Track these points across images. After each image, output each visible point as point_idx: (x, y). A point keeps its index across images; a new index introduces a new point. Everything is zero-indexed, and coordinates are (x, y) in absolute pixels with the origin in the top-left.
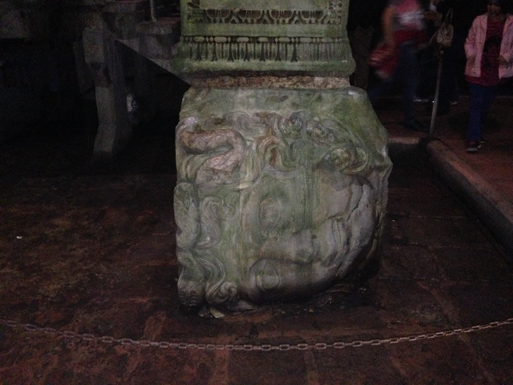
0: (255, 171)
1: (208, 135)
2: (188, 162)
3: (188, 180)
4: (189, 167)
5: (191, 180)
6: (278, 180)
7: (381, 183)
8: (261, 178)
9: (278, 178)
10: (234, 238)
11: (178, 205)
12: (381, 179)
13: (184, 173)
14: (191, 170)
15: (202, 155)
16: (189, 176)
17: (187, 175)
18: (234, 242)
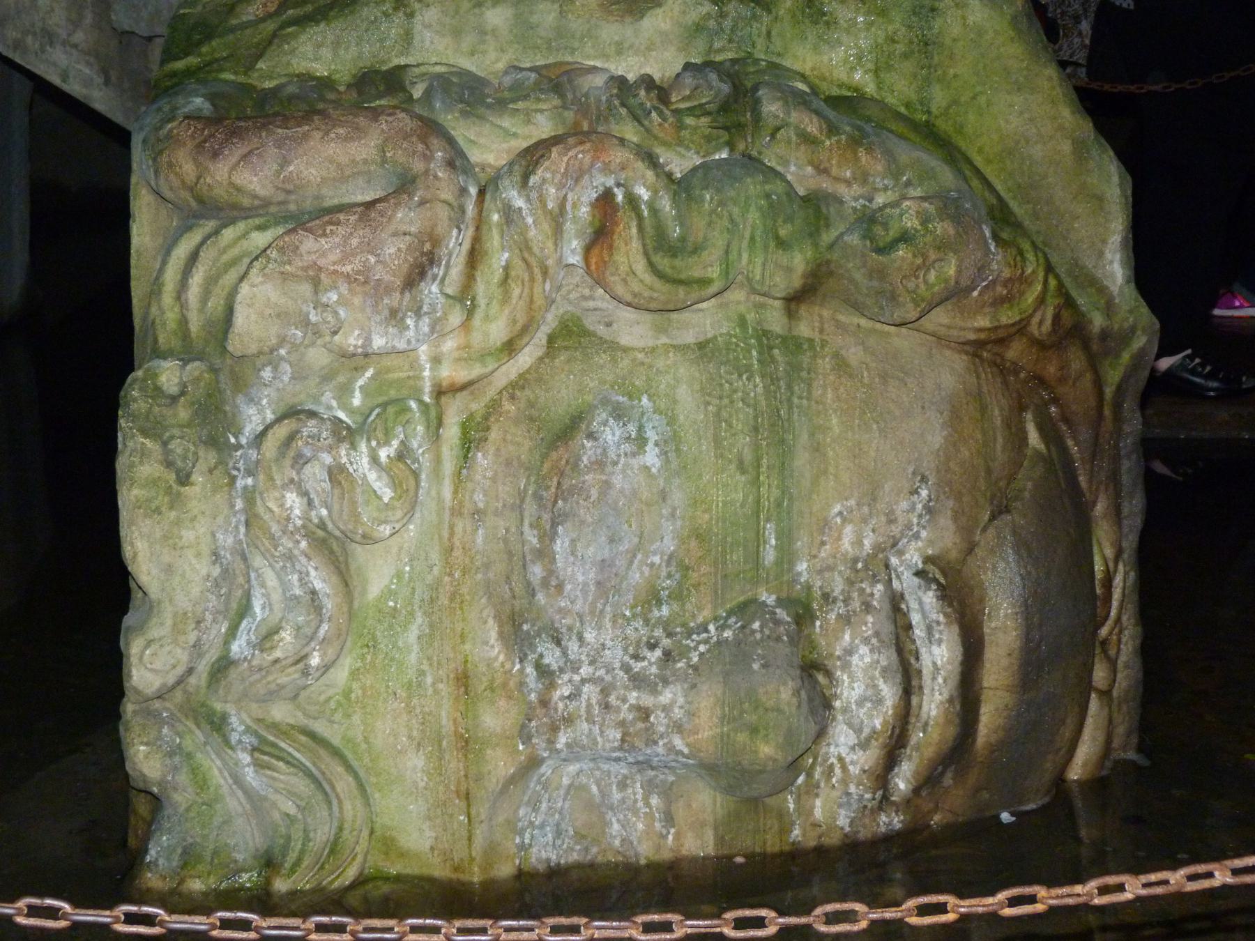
0: (516, 292)
1: (292, 123)
2: (194, 257)
3: (187, 353)
4: (197, 280)
5: (213, 342)
6: (625, 350)
7: (1107, 412)
8: (541, 337)
9: (625, 340)
10: (412, 635)
11: (139, 470)
12: (1109, 392)
13: (171, 316)
14: (204, 299)
15: (257, 221)
16: (194, 327)
17: (183, 321)
18: (413, 658)
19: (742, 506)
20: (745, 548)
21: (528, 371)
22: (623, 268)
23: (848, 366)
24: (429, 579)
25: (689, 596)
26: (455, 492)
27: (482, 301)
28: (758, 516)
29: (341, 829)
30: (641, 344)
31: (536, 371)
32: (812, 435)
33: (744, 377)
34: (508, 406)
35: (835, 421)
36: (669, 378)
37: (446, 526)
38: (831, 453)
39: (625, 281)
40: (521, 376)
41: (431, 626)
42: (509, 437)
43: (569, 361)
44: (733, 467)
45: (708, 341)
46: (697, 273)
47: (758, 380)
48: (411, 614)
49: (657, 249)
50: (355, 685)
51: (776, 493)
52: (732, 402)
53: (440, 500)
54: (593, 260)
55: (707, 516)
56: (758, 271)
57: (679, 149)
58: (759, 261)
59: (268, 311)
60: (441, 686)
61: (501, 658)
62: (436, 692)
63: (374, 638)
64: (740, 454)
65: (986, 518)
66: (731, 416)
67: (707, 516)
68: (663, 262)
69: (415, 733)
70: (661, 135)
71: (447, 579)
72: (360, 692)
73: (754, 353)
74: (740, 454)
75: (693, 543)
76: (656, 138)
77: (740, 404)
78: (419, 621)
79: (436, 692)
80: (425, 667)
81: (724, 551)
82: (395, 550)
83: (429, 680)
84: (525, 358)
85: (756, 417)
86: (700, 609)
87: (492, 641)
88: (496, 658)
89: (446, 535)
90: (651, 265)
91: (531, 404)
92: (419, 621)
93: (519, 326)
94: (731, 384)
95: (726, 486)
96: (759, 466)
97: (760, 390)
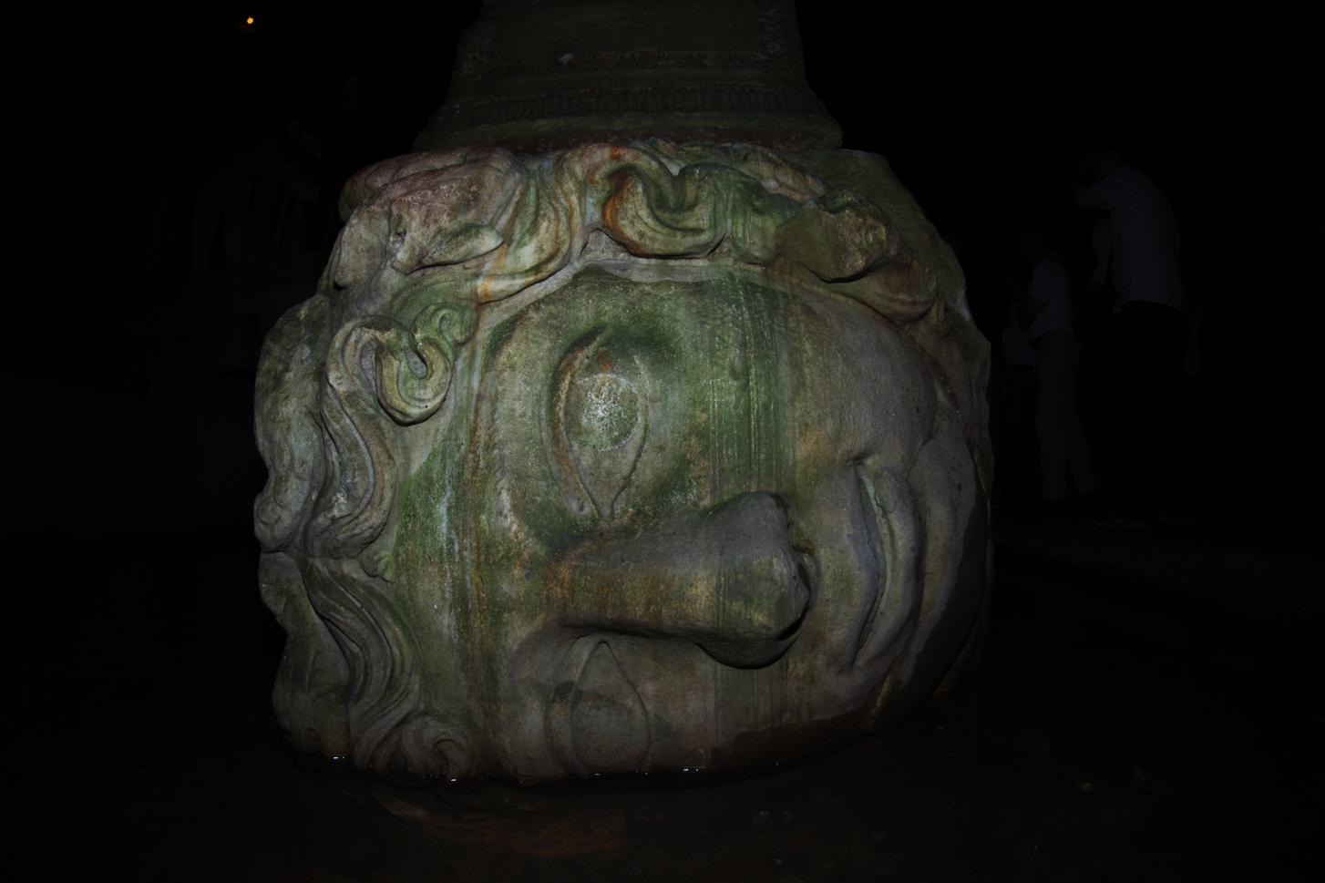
6: (636, 284)
19: (735, 408)
20: (740, 445)
21: (554, 293)
22: (631, 213)
23: (814, 313)
24: (457, 457)
25: (690, 487)
26: (482, 381)
27: (517, 237)
28: (749, 417)
29: (393, 671)
30: (650, 280)
31: (561, 293)
32: (791, 354)
33: (733, 306)
34: (531, 313)
35: (808, 346)
36: (671, 303)
37: (473, 410)
38: (807, 370)
39: (632, 222)
40: (547, 296)
41: (458, 499)
42: (530, 337)
43: (589, 289)
44: (727, 372)
45: (703, 283)
46: (691, 223)
47: (744, 309)
48: (443, 488)
49: (659, 207)
50: (401, 550)
51: (763, 397)
52: (724, 323)
53: (470, 388)
54: (608, 212)
55: (705, 416)
56: (740, 230)
57: (678, 161)
58: (741, 221)
59: (361, 247)
60: (466, 553)
61: (515, 527)
62: (462, 558)
63: (414, 509)
64: (732, 363)
65: (920, 443)
66: (723, 333)
67: (705, 416)
68: (666, 216)
69: (447, 595)
70: (665, 152)
71: (471, 456)
72: (404, 556)
73: (741, 293)
74: (732, 363)
75: (693, 440)
76: (661, 153)
77: (731, 325)
78: (449, 494)
79: (462, 558)
80: (453, 536)
81: (721, 446)
82: (432, 432)
83: (457, 548)
84: (552, 285)
85: (744, 336)
86: (701, 499)
87: (505, 512)
88: (510, 528)
89: (472, 417)
90: (657, 219)
91: (552, 316)
92: (449, 494)
93: (544, 256)
94: (723, 311)
95: (720, 389)
96: (748, 375)
97: (746, 316)
